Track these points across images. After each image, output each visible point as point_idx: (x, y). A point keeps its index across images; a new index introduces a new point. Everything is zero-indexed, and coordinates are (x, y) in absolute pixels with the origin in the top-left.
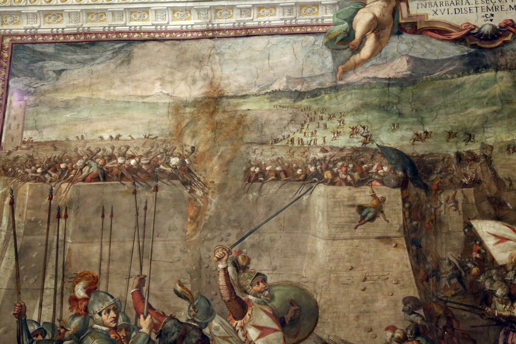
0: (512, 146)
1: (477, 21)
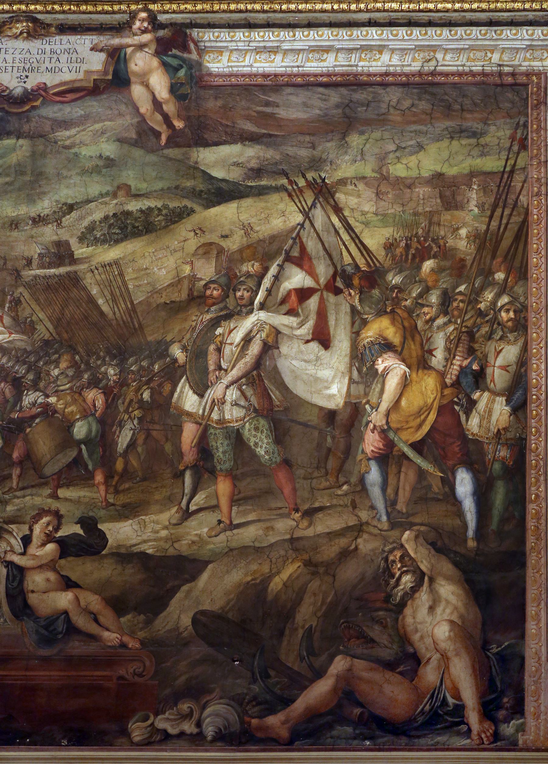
0: (15, 222)
1: (10, 82)
